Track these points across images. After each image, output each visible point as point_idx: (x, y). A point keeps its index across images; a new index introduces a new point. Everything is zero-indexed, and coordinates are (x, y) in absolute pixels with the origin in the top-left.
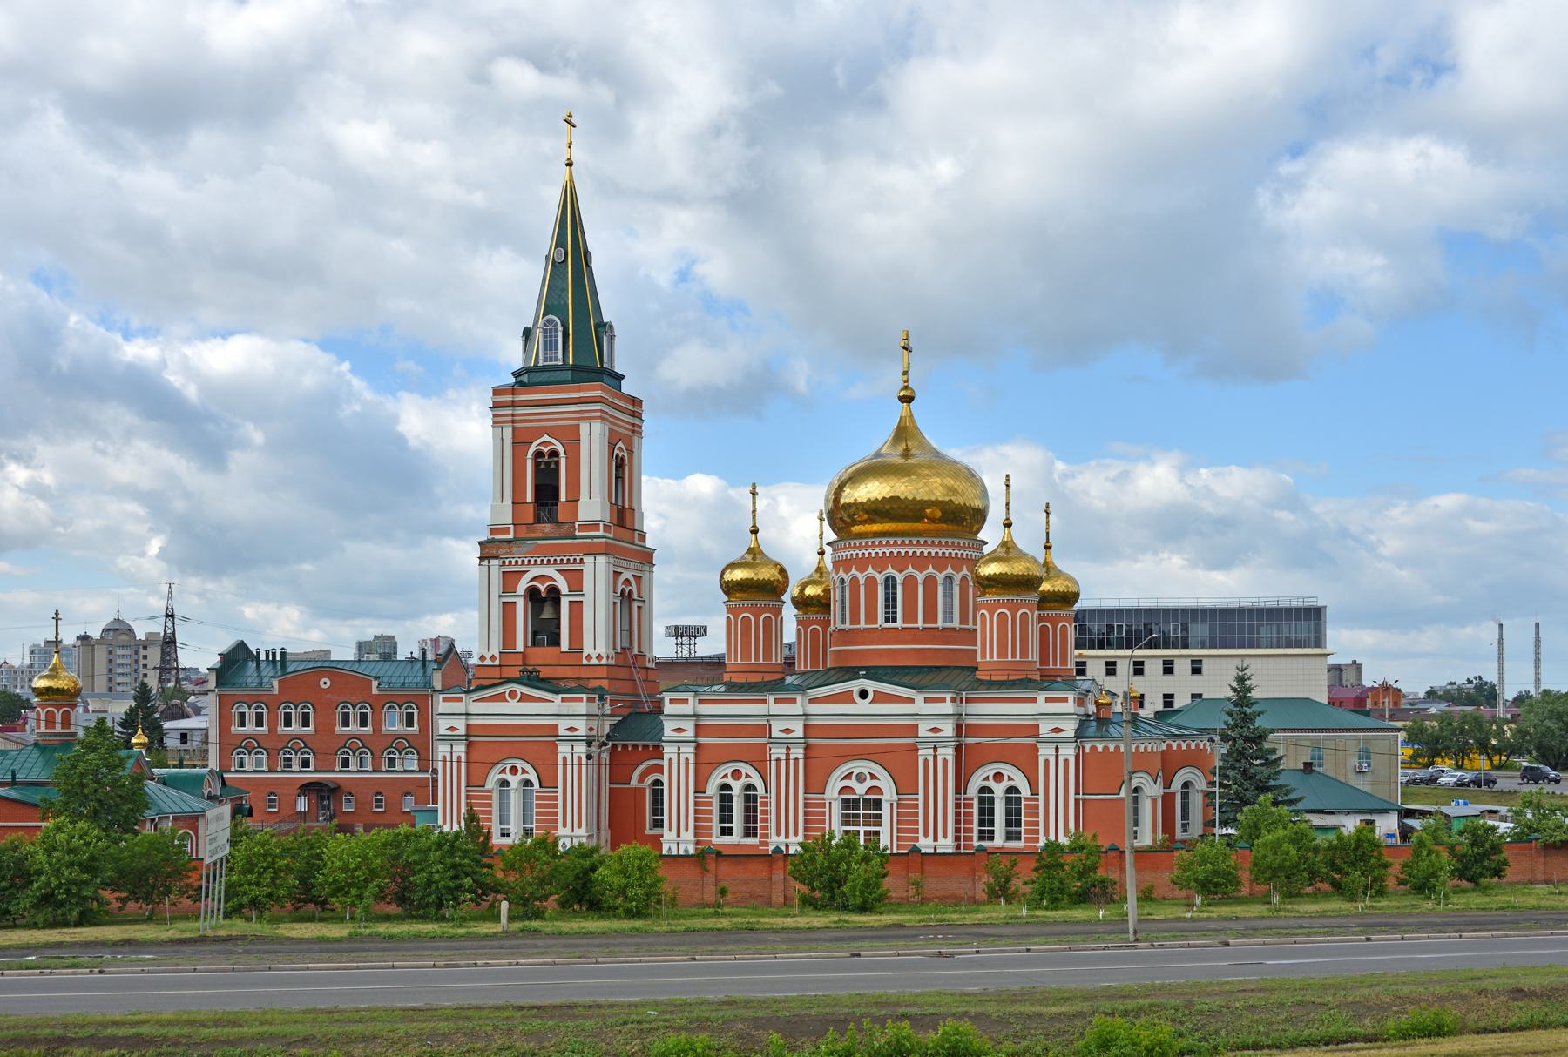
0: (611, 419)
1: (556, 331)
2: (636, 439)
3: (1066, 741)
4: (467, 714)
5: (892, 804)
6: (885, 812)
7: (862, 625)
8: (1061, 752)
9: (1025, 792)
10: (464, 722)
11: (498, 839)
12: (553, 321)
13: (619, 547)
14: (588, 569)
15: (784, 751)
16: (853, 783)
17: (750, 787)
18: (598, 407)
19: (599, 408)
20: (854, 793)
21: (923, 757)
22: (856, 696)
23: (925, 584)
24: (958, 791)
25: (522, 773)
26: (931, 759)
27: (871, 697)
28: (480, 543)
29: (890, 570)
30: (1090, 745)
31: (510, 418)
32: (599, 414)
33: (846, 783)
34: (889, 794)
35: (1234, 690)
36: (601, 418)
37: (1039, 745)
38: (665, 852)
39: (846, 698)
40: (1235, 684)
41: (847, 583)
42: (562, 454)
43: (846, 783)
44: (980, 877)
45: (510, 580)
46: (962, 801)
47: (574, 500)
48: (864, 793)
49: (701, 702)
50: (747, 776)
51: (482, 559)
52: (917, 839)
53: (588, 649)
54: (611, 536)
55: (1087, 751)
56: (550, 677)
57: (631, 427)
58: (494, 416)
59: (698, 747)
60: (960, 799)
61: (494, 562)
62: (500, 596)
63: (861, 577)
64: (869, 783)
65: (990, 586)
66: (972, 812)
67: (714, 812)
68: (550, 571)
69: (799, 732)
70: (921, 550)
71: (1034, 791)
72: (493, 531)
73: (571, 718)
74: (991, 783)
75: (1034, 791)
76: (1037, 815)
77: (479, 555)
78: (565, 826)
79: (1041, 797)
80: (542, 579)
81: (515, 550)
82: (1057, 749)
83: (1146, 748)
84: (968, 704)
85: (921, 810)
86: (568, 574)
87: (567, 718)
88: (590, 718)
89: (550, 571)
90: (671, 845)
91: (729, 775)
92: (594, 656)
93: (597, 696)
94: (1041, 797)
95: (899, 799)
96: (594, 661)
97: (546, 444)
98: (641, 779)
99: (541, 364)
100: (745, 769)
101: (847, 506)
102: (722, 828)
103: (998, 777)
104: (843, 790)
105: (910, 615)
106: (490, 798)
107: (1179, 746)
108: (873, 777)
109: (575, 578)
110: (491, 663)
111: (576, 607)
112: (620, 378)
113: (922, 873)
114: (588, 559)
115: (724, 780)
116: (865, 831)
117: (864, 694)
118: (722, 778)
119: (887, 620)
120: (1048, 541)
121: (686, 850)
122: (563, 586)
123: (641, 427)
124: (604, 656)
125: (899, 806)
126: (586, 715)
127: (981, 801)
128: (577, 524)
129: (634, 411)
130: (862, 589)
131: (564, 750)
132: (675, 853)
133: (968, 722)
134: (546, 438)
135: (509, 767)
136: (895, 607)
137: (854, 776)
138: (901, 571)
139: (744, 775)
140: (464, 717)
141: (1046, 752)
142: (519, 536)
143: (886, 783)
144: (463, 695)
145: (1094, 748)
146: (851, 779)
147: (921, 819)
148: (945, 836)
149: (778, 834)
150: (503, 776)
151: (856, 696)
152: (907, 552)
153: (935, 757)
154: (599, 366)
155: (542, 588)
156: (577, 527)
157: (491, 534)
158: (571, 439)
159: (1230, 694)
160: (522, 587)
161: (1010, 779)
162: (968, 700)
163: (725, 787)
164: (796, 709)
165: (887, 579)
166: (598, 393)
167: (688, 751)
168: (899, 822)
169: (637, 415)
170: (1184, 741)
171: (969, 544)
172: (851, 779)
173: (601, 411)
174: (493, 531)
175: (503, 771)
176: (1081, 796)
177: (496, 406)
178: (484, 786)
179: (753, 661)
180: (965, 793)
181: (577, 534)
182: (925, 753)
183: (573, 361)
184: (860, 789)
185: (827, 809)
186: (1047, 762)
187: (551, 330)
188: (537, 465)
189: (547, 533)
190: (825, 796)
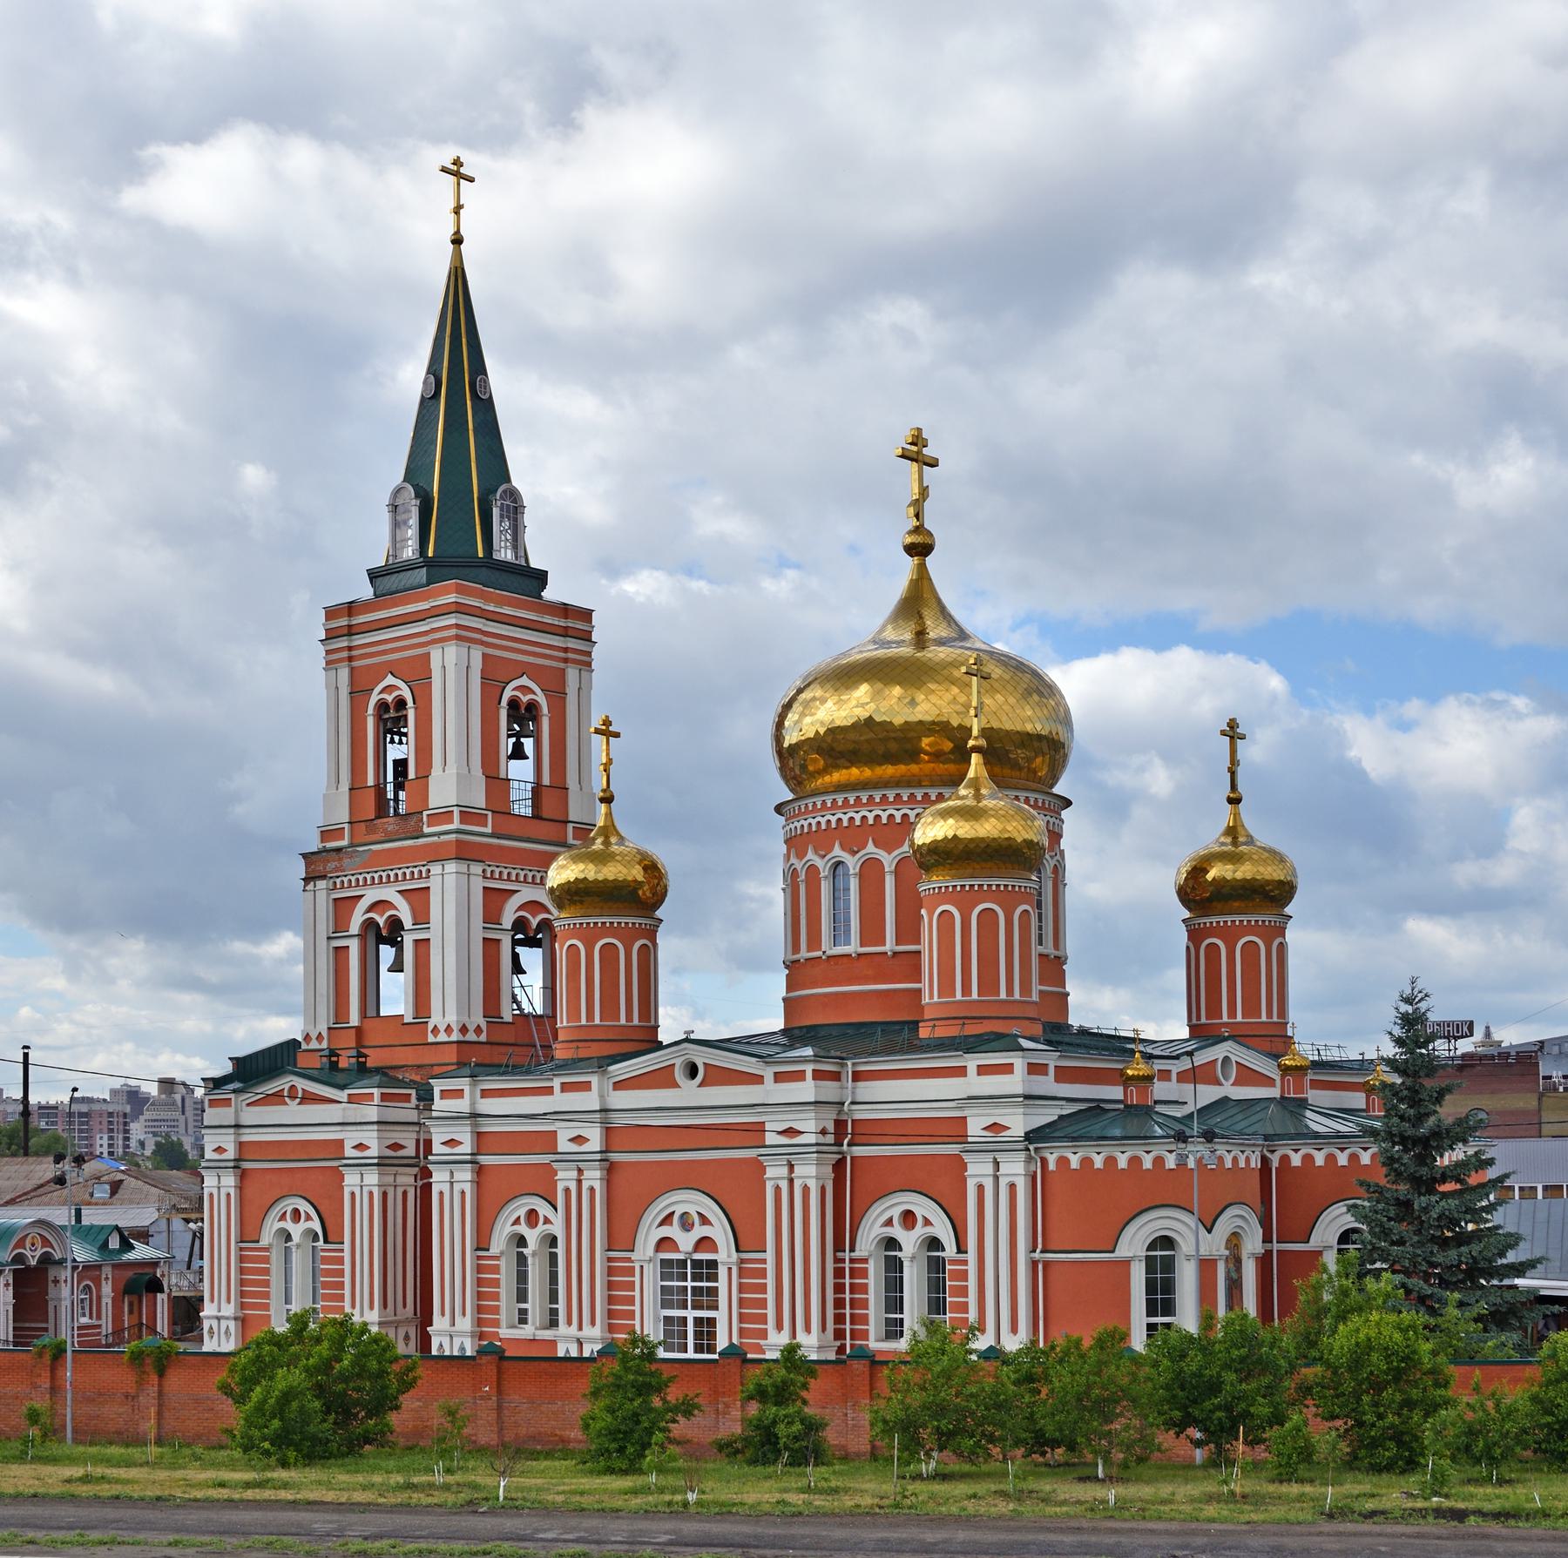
0: (485, 639)
2: (572, 674)
3: (1008, 1148)
4: (237, 1126)
5: (730, 1269)
8: (1003, 1169)
9: (950, 1250)
10: (232, 1138)
11: (513, 1327)
13: (501, 848)
14: (434, 884)
15: (574, 1174)
16: (674, 1231)
17: (934, 1243)
18: (451, 620)
19: (453, 621)
20: (677, 1250)
21: (772, 1182)
22: (679, 1075)
23: (861, 875)
24: (839, 1246)
25: (544, 1223)
26: (784, 1185)
28: (305, 856)
29: (838, 852)
30: (1055, 1155)
31: (345, 654)
32: (453, 632)
33: (665, 1231)
34: (725, 1254)
35: (1399, 1042)
36: (458, 637)
37: (967, 1158)
38: (434, 1352)
40: (1397, 1031)
41: (803, 876)
42: (410, 703)
43: (665, 1231)
44: (727, 1406)
46: (847, 1265)
48: (690, 1248)
49: (485, 1094)
51: (307, 880)
53: (436, 1019)
54: (489, 830)
55: (1052, 1166)
56: (389, 1064)
57: (562, 655)
58: (328, 652)
59: (480, 1170)
60: (843, 1261)
61: (321, 884)
62: (329, 938)
64: (699, 1231)
65: (937, 864)
66: (866, 1285)
67: (503, 1283)
68: (390, 893)
69: (595, 1142)
70: (888, 813)
71: (961, 1249)
72: (326, 834)
73: (359, 1128)
74: (897, 1232)
75: (961, 1249)
77: (303, 876)
79: (972, 1256)
80: (381, 906)
81: (346, 862)
82: (997, 1164)
83: (1235, 1160)
84: (860, 1084)
85: (770, 1281)
86: (407, 894)
87: (354, 1128)
88: (383, 1127)
89: (390, 893)
90: (464, 1340)
91: (895, 1221)
93: (413, 1092)
94: (972, 1256)
95: (742, 1261)
96: (442, 1037)
97: (389, 689)
100: (922, 1207)
101: (794, 748)
103: (908, 1218)
104: (664, 1243)
106: (266, 1260)
107: (1331, 1158)
112: (541, 578)
113: (872, 1398)
114: (436, 869)
115: (515, 1227)
116: (695, 1318)
118: (661, 1224)
120: (1234, 787)
121: (462, 1349)
123: (589, 654)
124: (455, 1028)
126: (378, 1123)
127: (1150, 1262)
128: (425, 813)
129: (566, 628)
131: (351, 1179)
132: (447, 1353)
133: (858, 1116)
134: (390, 680)
135: (289, 1209)
137: (676, 1218)
138: (854, 853)
139: (541, 1220)
140: (232, 1131)
141: (978, 1169)
142: (356, 841)
144: (232, 1096)
145: (1063, 1161)
146: (671, 1224)
147: (770, 1296)
150: (282, 1224)
151: (679, 1075)
152: (852, 819)
154: (481, 554)
155: (381, 921)
156: (425, 819)
157: (322, 842)
159: (1390, 1050)
162: (857, 1076)
163: (892, 1243)
164: (589, 1101)
166: (451, 598)
168: (741, 1302)
169: (586, 637)
170: (1342, 1150)
171: (1043, 803)
172: (671, 1224)
173: (458, 626)
174: (326, 834)
175: (283, 1217)
176: (1037, 1255)
177: (331, 635)
178: (258, 1242)
179: (584, 1022)
180: (852, 1249)
181: (426, 830)
182: (775, 1172)
183: (434, 552)
186: (981, 1188)
189: (391, 832)
190: (634, 1256)
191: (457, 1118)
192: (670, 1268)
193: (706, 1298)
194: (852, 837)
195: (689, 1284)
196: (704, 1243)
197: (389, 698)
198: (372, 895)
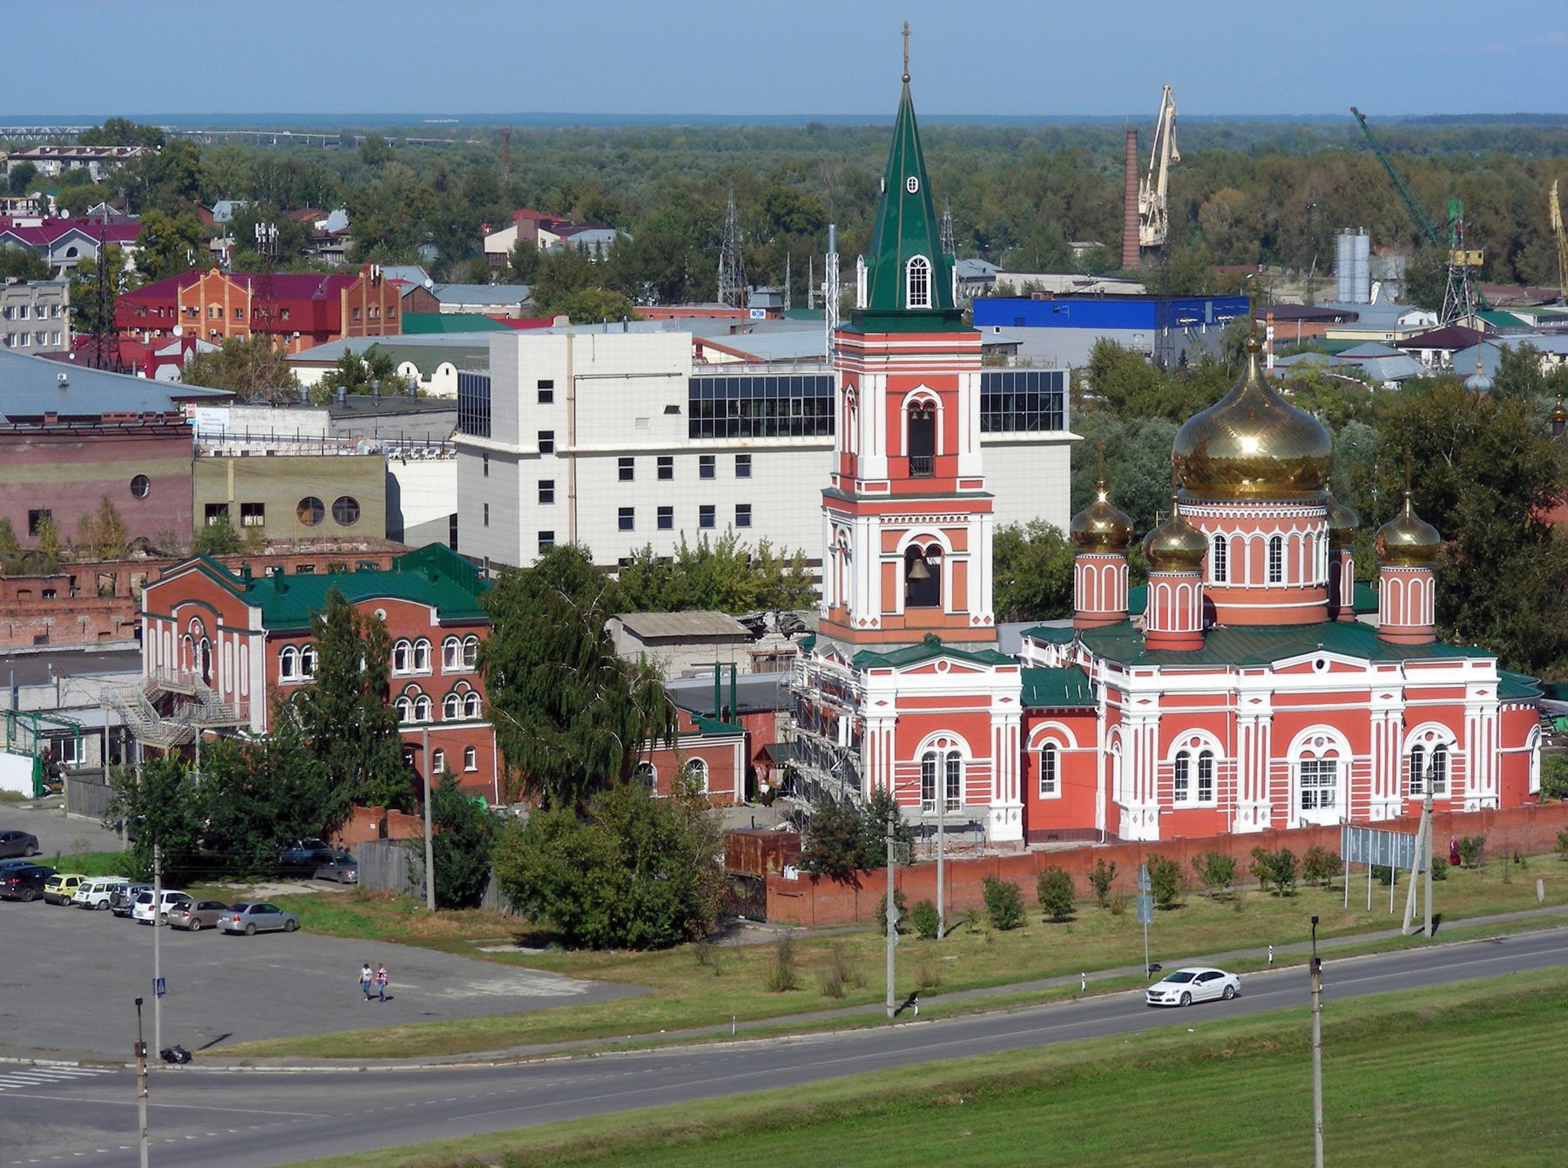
1: (924, 272)
6: (1340, 771)
7: (1247, 584)
12: (921, 261)
16: (1312, 747)
27: (1327, 666)
39: (1305, 668)
45: (890, 538)
47: (952, 453)
50: (1206, 743)
52: (1368, 796)
61: (875, 520)
63: (1247, 538)
64: (1327, 746)
68: (933, 529)
76: (1463, 769)
78: (998, 797)
89: (933, 529)
92: (982, 618)
97: (922, 394)
98: (1035, 744)
99: (909, 306)
102: (1201, 793)
105: (1293, 576)
108: (1330, 740)
109: (959, 537)
110: (871, 627)
111: (960, 567)
117: (1320, 664)
119: (1272, 579)
122: (945, 543)
125: (1354, 767)
130: (1247, 550)
134: (922, 388)
136: (1279, 566)
143: (1342, 745)
148: (1394, 792)
149: (1246, 797)
153: (1386, 721)
158: (949, 389)
160: (902, 546)
161: (1440, 737)
165: (1273, 540)
175: (931, 744)
181: (959, 490)
184: (1319, 752)
185: (1290, 773)
187: (918, 270)
188: (910, 415)
192: (1305, 767)
194: (1267, 524)
195: (1319, 774)
197: (922, 400)
198: (916, 530)
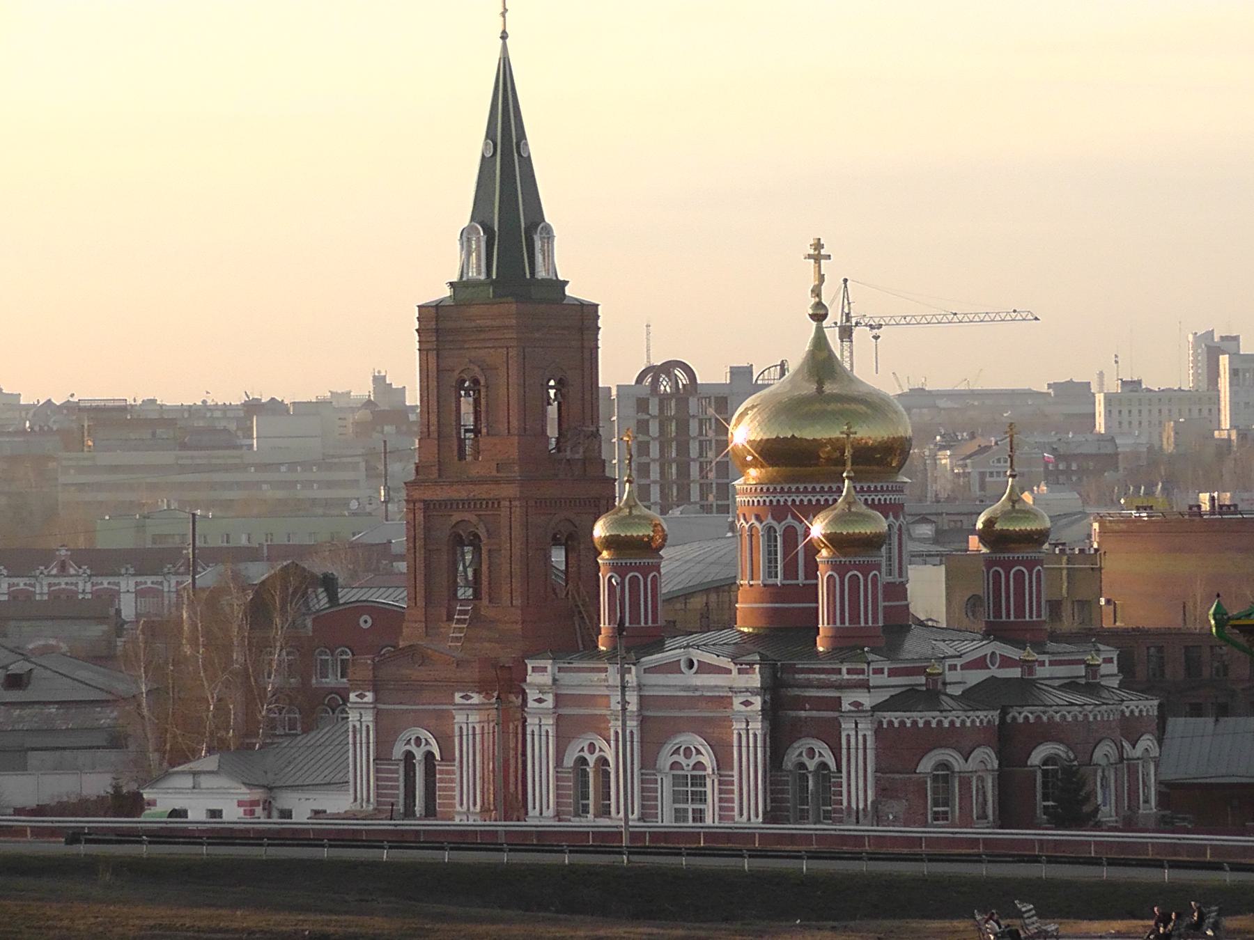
16: (680, 758)
33: (676, 758)
37: (841, 720)
85: (736, 788)
103: (811, 753)
104: (675, 765)
135: (413, 738)
141: (847, 727)
150: (408, 747)
154: (528, 276)
167: (548, 723)
186: (848, 736)
191: (541, 688)
192: (678, 780)
193: (701, 797)
195: (689, 789)
196: (699, 766)
